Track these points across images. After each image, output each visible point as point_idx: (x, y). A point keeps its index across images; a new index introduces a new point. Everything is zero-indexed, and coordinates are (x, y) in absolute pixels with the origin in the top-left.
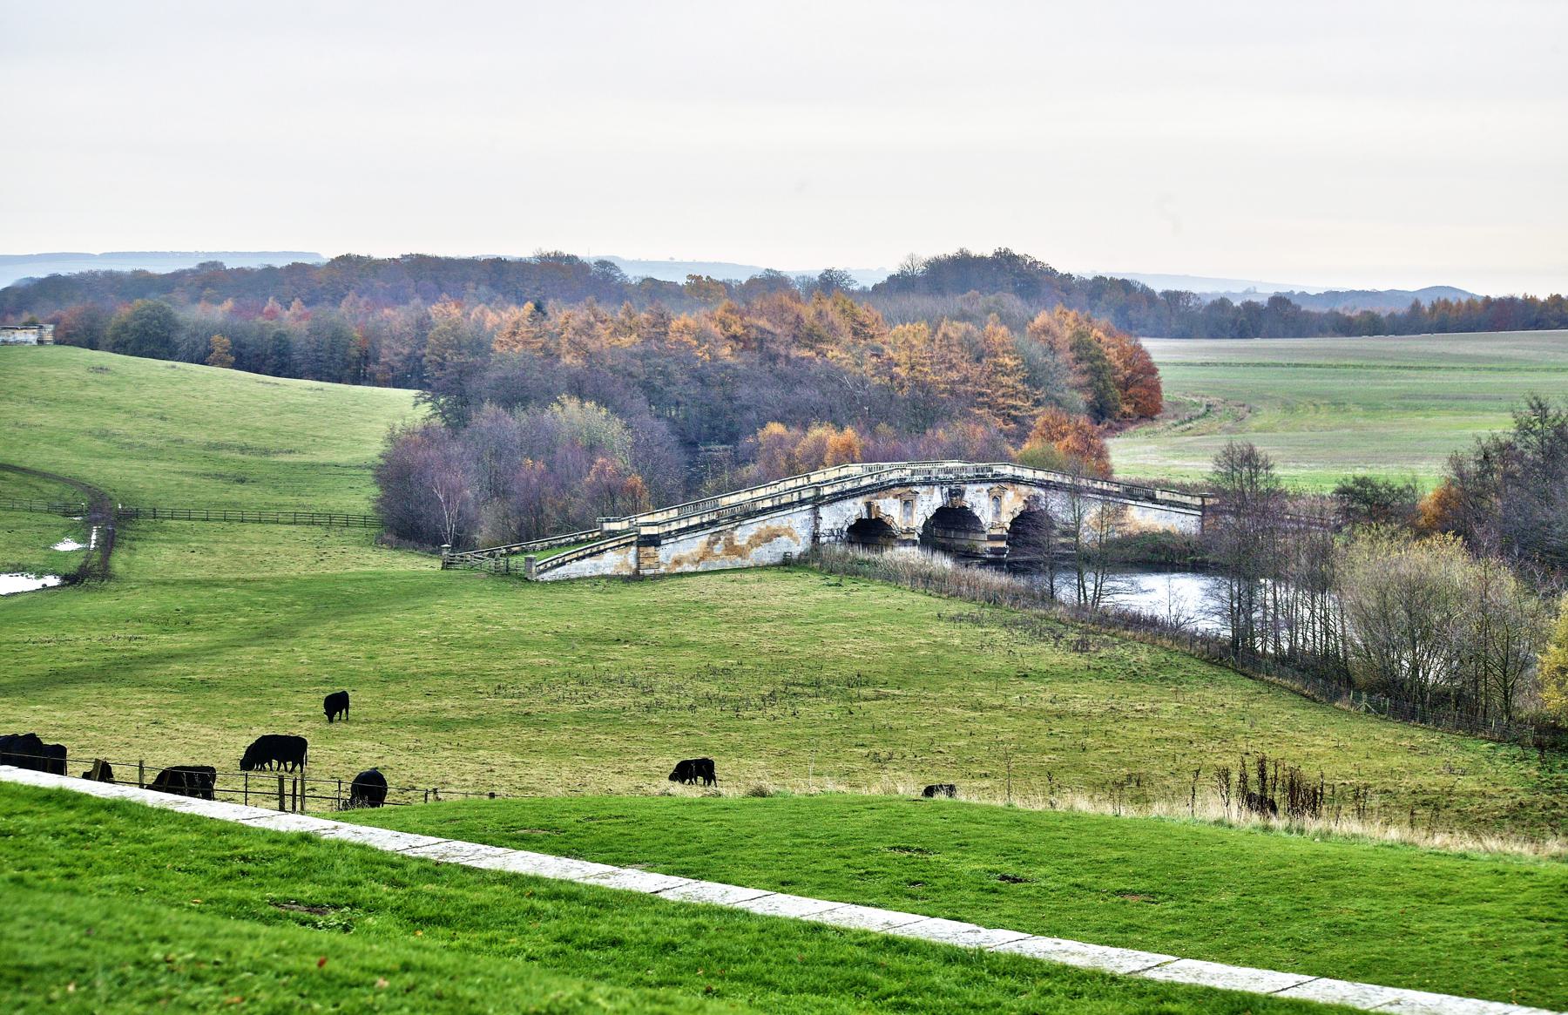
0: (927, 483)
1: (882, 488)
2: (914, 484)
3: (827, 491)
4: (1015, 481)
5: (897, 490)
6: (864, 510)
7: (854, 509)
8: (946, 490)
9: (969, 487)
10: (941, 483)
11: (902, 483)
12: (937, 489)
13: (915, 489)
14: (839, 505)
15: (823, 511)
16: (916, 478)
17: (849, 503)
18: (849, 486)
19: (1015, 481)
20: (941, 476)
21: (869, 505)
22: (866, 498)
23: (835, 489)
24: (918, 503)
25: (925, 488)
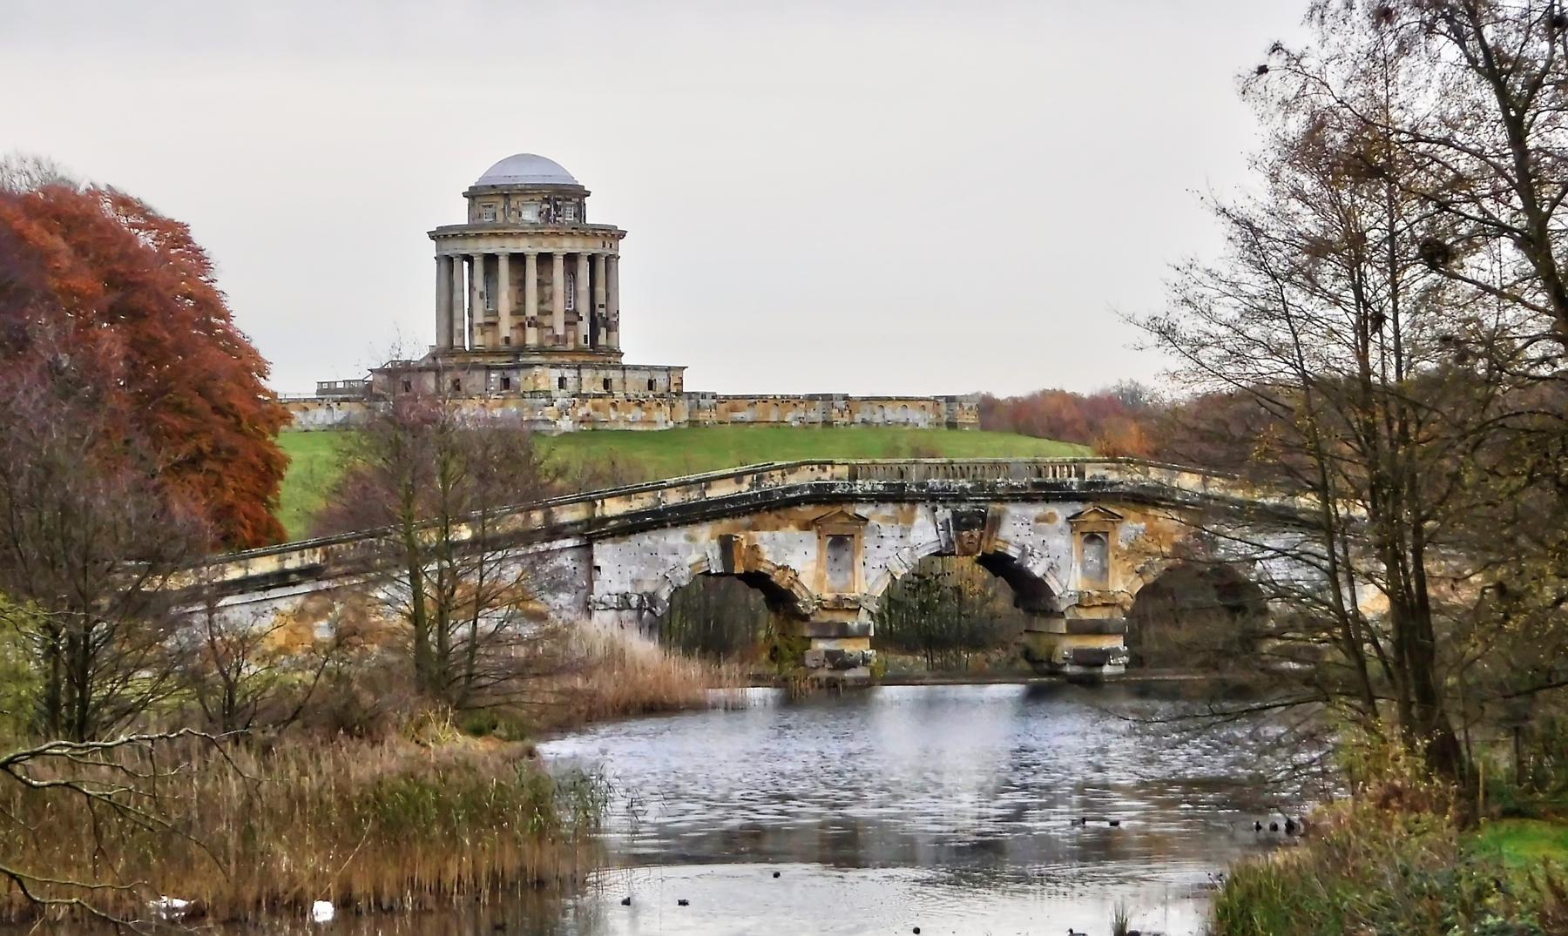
0: (895, 495)
1: (768, 506)
2: (853, 498)
3: (614, 507)
4: (1143, 499)
5: (808, 512)
6: (715, 554)
7: (691, 551)
8: (944, 513)
9: (1014, 510)
10: (933, 498)
11: (821, 496)
12: (921, 512)
13: (863, 510)
14: (647, 540)
15: (604, 553)
16: (861, 486)
17: (675, 538)
18: (673, 498)
19: (1143, 499)
20: (934, 482)
21: (727, 544)
22: (725, 526)
23: (636, 505)
24: (868, 541)
25: (888, 510)
